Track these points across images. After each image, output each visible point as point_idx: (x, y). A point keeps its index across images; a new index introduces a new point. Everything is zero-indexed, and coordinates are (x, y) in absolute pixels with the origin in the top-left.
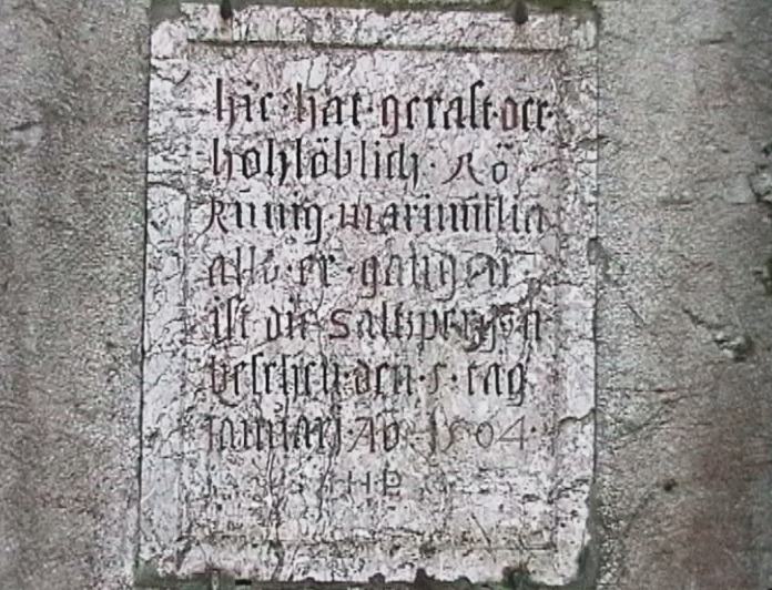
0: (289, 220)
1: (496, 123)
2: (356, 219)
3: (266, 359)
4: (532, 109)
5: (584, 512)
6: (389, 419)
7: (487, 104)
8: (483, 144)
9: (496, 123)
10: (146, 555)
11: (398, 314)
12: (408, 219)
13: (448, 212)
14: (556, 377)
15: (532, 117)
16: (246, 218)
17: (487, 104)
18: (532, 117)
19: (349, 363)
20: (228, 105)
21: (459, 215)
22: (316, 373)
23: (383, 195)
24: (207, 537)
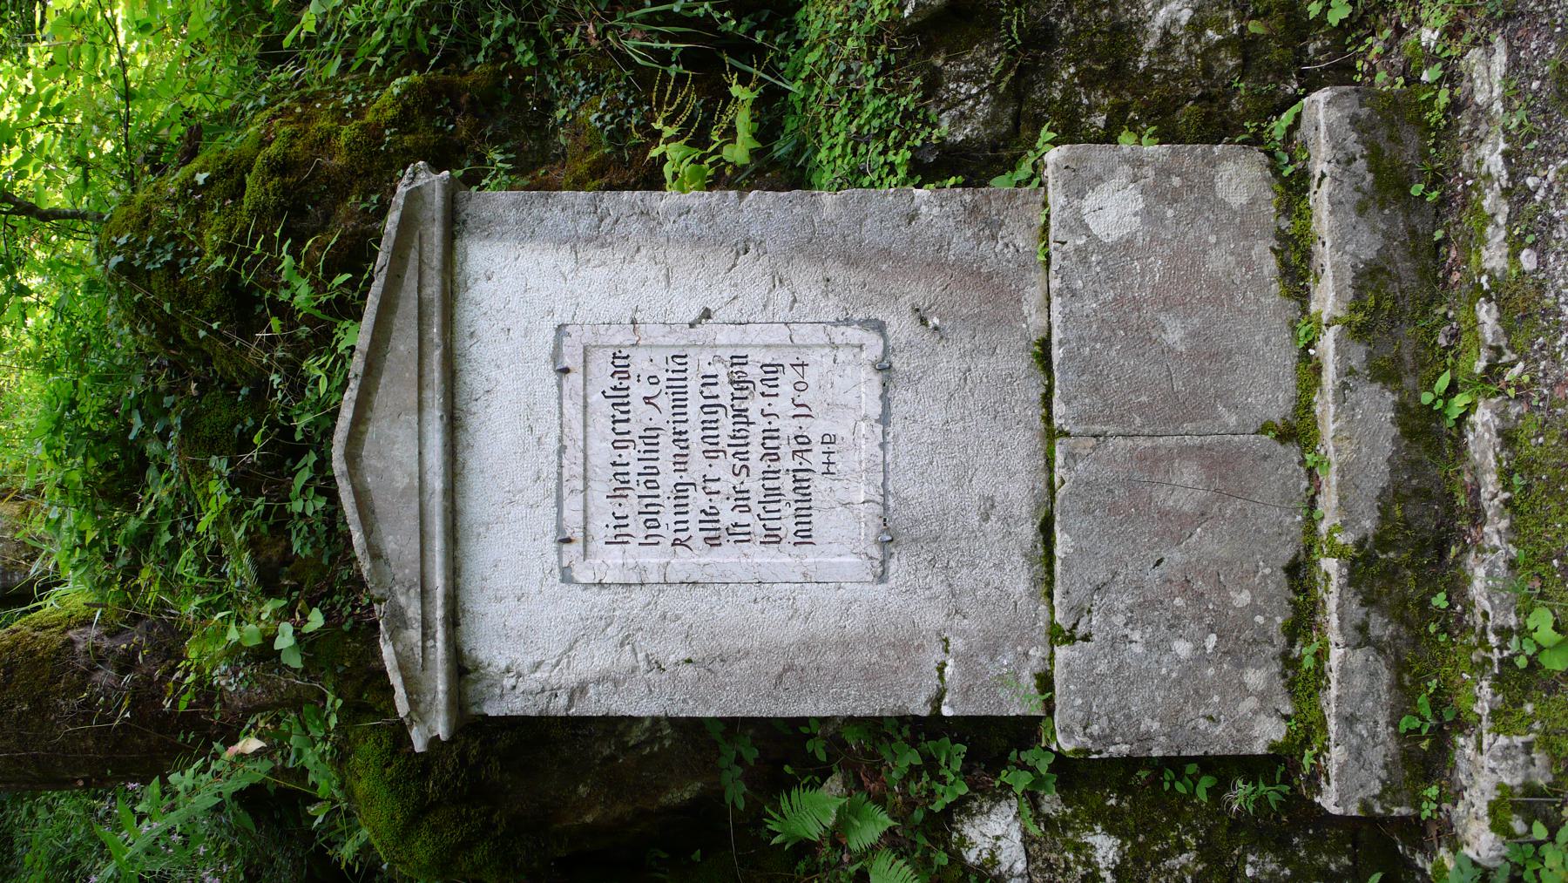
0: (683, 501)
1: (625, 384)
2: (681, 462)
3: (762, 513)
4: (618, 362)
5: (843, 329)
6: (793, 442)
7: (615, 389)
8: (638, 390)
9: (625, 384)
10: (870, 578)
11: (734, 437)
12: (680, 433)
13: (677, 410)
14: (768, 346)
15: (622, 362)
16: (683, 526)
17: (615, 389)
18: (622, 362)
19: (764, 466)
20: (619, 540)
21: (679, 404)
22: (769, 484)
23: (667, 448)
24: (855, 784)
